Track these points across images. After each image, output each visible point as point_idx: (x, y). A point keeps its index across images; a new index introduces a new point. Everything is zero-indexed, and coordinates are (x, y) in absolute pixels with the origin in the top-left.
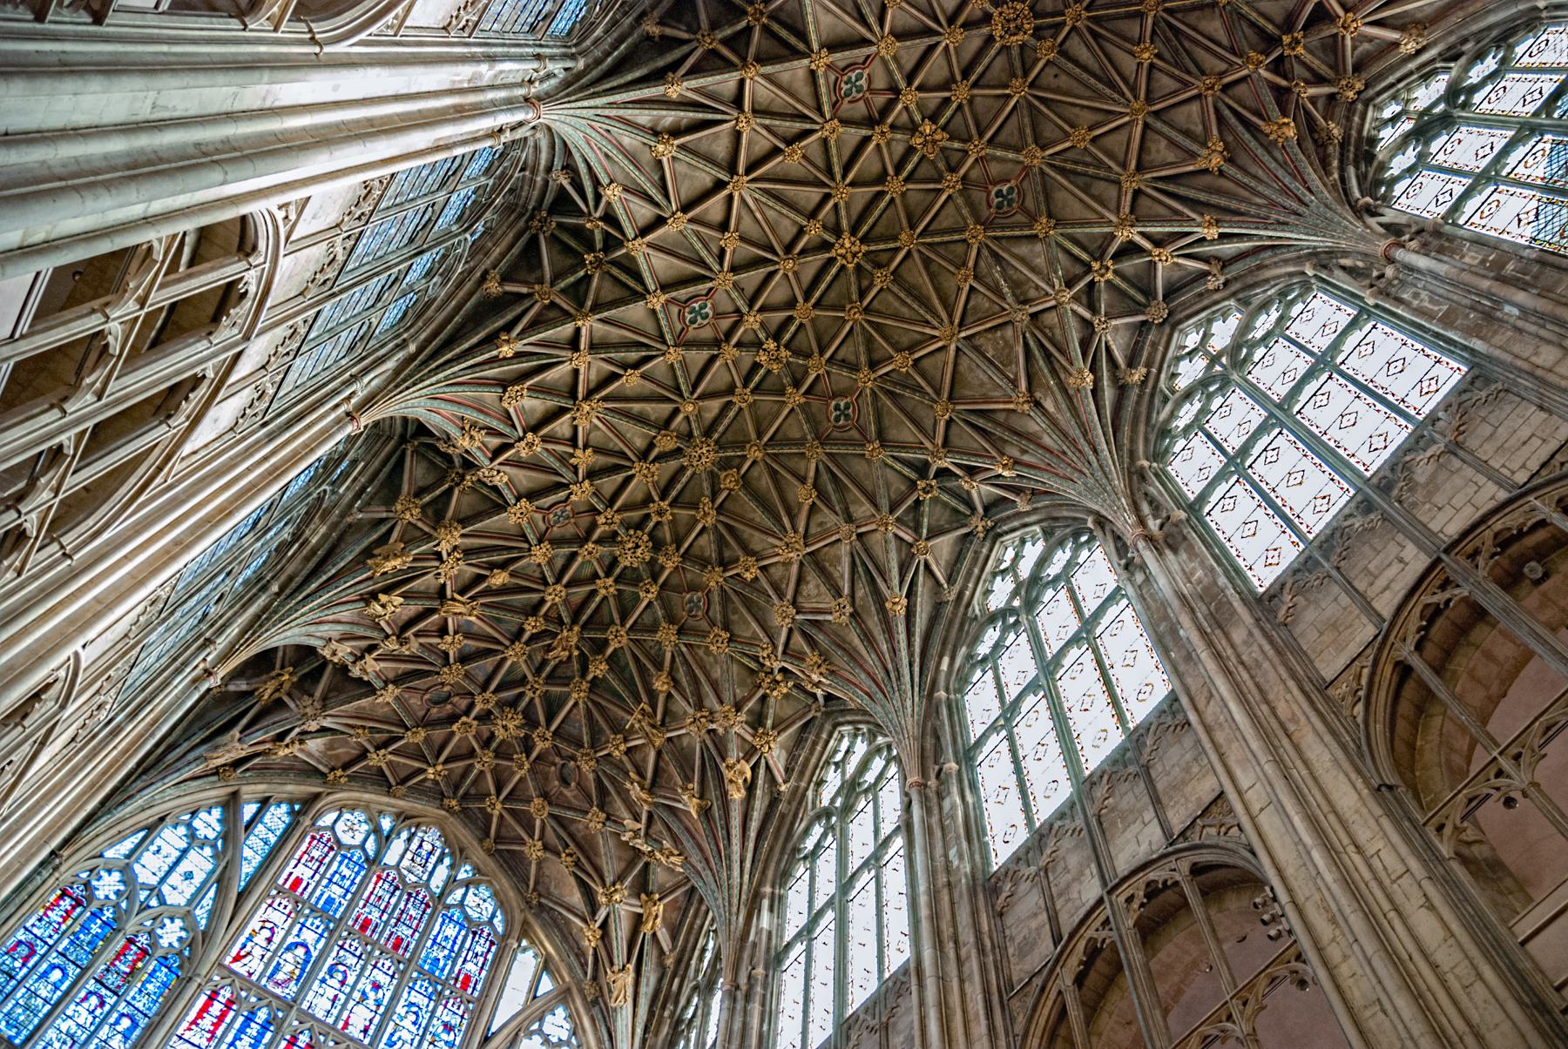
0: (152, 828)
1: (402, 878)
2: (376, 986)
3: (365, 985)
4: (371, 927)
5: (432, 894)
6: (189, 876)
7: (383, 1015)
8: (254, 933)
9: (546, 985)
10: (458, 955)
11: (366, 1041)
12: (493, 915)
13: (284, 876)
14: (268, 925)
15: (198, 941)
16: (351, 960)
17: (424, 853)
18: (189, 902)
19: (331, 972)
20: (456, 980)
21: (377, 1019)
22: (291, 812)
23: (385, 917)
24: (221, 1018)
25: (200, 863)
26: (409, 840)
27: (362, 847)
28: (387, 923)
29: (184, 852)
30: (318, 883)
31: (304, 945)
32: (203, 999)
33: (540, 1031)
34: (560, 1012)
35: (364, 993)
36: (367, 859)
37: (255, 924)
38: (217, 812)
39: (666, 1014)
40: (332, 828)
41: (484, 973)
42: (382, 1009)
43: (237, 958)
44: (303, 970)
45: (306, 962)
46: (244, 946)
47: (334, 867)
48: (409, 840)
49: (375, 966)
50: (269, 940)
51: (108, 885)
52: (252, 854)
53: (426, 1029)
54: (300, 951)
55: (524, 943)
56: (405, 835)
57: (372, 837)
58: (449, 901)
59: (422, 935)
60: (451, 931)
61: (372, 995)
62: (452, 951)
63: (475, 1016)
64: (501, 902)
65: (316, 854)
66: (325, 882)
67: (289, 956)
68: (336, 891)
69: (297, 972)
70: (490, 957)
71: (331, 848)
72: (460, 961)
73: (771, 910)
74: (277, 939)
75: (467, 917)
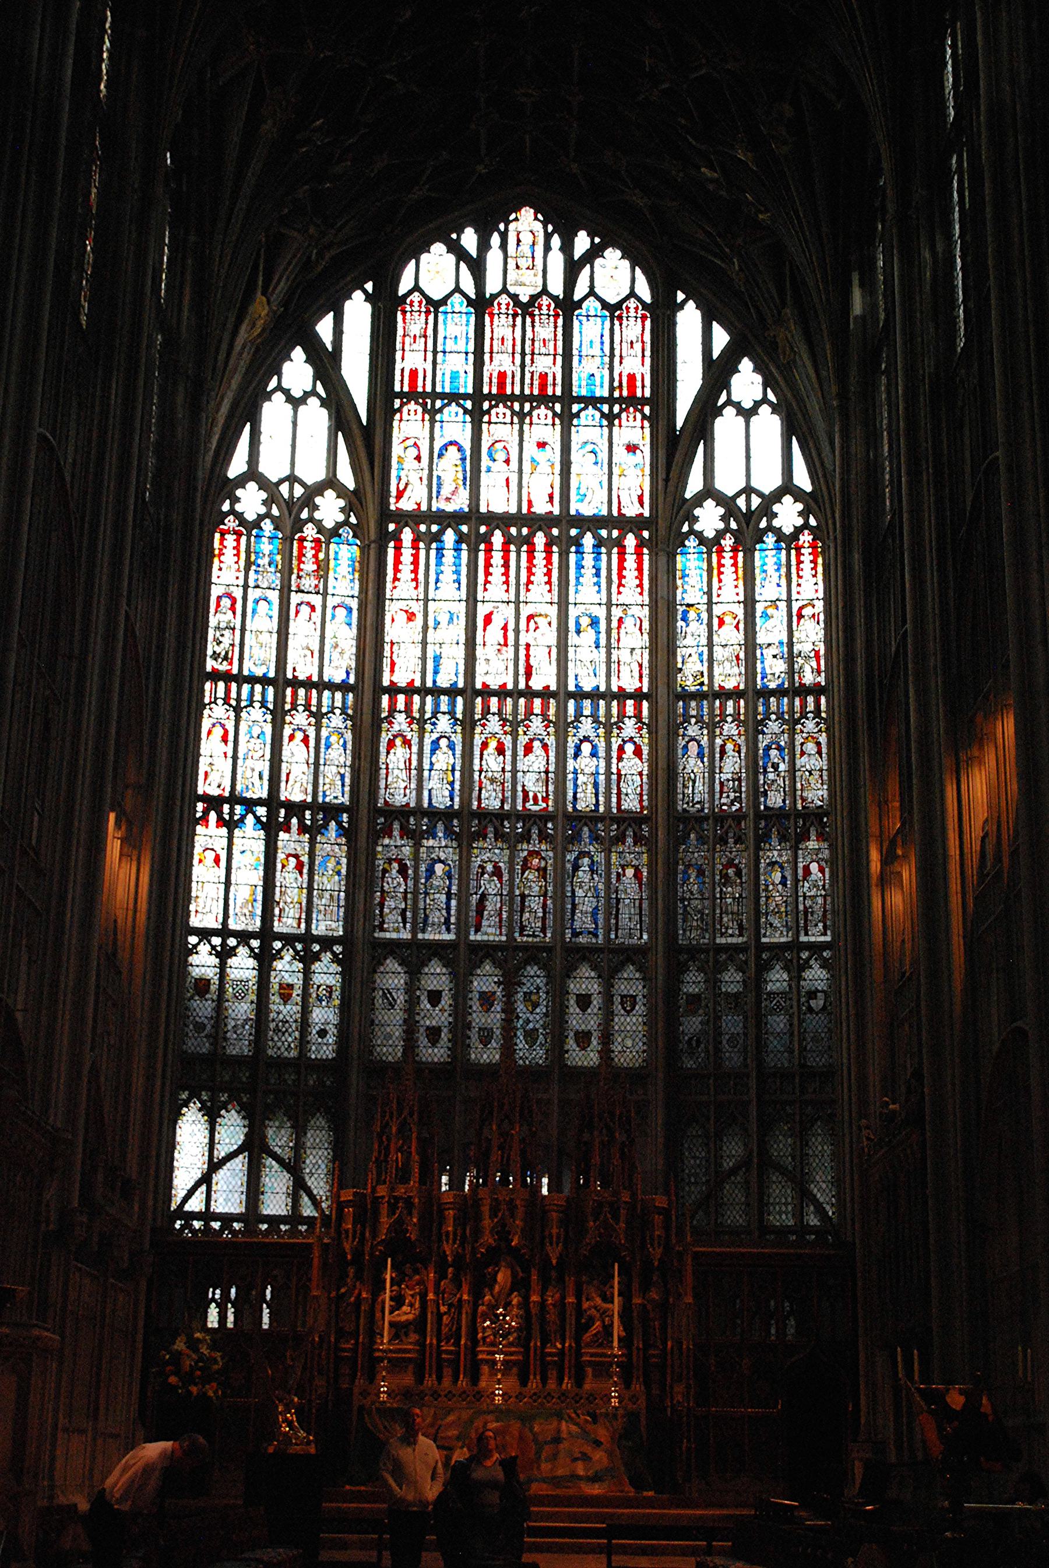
0: (254, 417)
1: (514, 297)
2: (542, 445)
3: (530, 448)
4: (509, 381)
5: (555, 298)
9: (721, 338)
10: (612, 356)
11: (556, 511)
14: (410, 442)
15: (353, 501)
17: (525, 249)
20: (620, 386)
22: (368, 298)
23: (518, 357)
24: (415, 562)
26: (504, 246)
27: (457, 289)
28: (523, 366)
33: (729, 402)
34: (746, 365)
35: (533, 460)
36: (470, 302)
37: (397, 450)
38: (298, 354)
40: (417, 288)
41: (648, 361)
43: (400, 495)
45: (463, 459)
46: (400, 479)
48: (504, 246)
50: (418, 458)
54: (452, 449)
55: (680, 296)
56: (495, 240)
57: (463, 266)
58: (577, 296)
63: (653, 420)
64: (634, 256)
65: (415, 329)
66: (440, 356)
69: (460, 476)
70: (647, 337)
71: (428, 312)
73: (862, 285)
75: (605, 305)
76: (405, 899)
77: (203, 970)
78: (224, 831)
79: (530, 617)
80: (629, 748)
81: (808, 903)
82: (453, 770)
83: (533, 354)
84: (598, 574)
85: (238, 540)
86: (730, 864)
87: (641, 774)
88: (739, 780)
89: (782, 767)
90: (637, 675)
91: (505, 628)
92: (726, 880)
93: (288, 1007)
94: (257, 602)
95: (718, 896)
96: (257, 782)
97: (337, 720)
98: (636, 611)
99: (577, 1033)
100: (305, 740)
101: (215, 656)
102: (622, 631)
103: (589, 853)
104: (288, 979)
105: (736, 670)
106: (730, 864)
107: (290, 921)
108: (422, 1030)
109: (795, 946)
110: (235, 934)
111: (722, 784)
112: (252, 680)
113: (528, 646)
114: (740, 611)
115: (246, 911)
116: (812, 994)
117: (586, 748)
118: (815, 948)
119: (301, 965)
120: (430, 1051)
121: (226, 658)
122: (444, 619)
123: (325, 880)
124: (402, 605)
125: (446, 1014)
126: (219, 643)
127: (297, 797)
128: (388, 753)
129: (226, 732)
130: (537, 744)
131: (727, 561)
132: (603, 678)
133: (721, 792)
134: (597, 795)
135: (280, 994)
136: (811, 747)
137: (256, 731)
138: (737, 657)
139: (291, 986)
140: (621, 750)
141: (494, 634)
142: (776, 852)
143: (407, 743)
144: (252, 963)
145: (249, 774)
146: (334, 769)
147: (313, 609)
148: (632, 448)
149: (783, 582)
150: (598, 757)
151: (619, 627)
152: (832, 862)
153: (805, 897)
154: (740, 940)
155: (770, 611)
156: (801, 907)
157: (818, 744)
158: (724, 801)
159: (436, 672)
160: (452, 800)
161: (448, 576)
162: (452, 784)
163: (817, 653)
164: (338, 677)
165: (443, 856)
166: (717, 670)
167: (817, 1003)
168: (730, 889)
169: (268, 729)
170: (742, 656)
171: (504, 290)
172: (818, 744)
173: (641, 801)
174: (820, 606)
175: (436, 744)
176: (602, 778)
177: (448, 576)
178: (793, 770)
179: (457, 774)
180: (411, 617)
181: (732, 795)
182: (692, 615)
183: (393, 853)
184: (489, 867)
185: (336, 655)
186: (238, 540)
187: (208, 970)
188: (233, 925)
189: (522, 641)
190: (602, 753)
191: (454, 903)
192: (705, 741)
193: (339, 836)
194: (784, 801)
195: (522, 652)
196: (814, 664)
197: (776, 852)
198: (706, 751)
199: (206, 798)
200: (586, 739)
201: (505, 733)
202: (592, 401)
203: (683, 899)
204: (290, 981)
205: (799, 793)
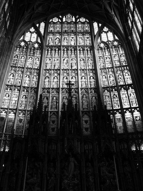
2: (73, 38)
6: (34, 37)
7: (76, 41)
8: (49, 41)
9: (100, 25)
11: (75, 45)
12: (86, 20)
13: (49, 31)
16: (66, 36)
18: (36, 40)
19: (64, 39)
21: (75, 42)
23: (68, 28)
25: (35, 35)
28: (69, 29)
29: (31, 35)
30: (55, 29)
31: (58, 38)
32: (47, 52)
33: (103, 31)
35: (71, 40)
37: (48, 39)
39: (123, 15)
40: (52, 21)
42: (75, 40)
44: (60, 41)
45: (59, 40)
46: (48, 42)
47: (56, 26)
49: (71, 35)
50: (52, 40)
51: (23, 44)
52: (42, 30)
53: (84, 40)
54: (58, 39)
56: (64, 17)
57: (59, 20)
59: (76, 28)
60: (80, 25)
61: (73, 39)
62: (82, 28)
65: (52, 26)
67: (56, 40)
68: (58, 29)
70: (89, 26)
72: (84, 29)
74: (53, 39)
76: (47, 103)
77: (3, 116)
78: (11, 91)
79: (71, 59)
80: (92, 78)
81: (132, 100)
82: (58, 82)
83: (71, 28)
84: (83, 53)
85: (20, 49)
86: (114, 95)
87: (94, 81)
88: (114, 81)
89: (122, 78)
90: (92, 67)
91: (67, 61)
92: (114, 98)
93: (21, 124)
94: (22, 57)
95: (113, 100)
96: (19, 83)
97: (35, 74)
98: (90, 58)
99: (85, 128)
100: (29, 77)
101: (13, 64)
102: (89, 61)
103: (85, 94)
104: (21, 118)
105: (110, 65)
106: (114, 95)
107: (23, 107)
108: (51, 128)
109: (131, 108)
110: (10, 109)
111: (110, 82)
112: (19, 67)
113: (71, 63)
114: (110, 56)
115: (14, 105)
116: (136, 117)
117: (83, 78)
118: (135, 108)
119: (24, 116)
120: (52, 133)
121: (15, 64)
122: (56, 60)
123: (31, 100)
124: (48, 58)
125: (56, 125)
126: (14, 62)
127: (26, 85)
128: (45, 79)
129: (13, 75)
130: (74, 77)
131: (106, 50)
132: (86, 67)
133: (111, 83)
134: (86, 85)
135: (20, 121)
136: (127, 74)
137: (19, 75)
138: (110, 63)
139: (22, 120)
140: (90, 78)
141: (65, 61)
142: (123, 92)
143: (49, 78)
144: (14, 115)
145: (17, 82)
146: (34, 82)
147: (32, 58)
148: (88, 38)
149: (117, 52)
150: (86, 79)
151: (88, 60)
152: (136, 92)
153: (131, 99)
154: (118, 108)
155: (115, 56)
156: (131, 101)
157: (128, 74)
158: (111, 84)
159: (54, 67)
160: (57, 86)
161: (57, 54)
162: (57, 84)
163: (125, 61)
164: (37, 68)
165: (55, 96)
166: (106, 65)
167: (138, 119)
168: (115, 99)
169: (22, 75)
170: (111, 62)
171: (66, 21)
172: (128, 74)
173: (95, 86)
174: (124, 54)
175: (54, 78)
176: (87, 82)
177: (57, 54)
178: (124, 78)
179: (58, 82)
180: (50, 60)
181: (113, 84)
182: (101, 58)
183: (45, 96)
184: (65, 98)
185: (36, 65)
186: (20, 49)
187: (4, 116)
188: (10, 107)
189: (70, 62)
190: (86, 78)
191: (58, 104)
192: (106, 76)
193: (34, 93)
194: (123, 83)
195: (70, 64)
196: (125, 62)
197: (123, 92)
198: (107, 77)
199: (8, 85)
200: (83, 76)
201: (68, 76)
202: (81, 33)
203: (105, 102)
204: (22, 119)
205: (126, 82)
